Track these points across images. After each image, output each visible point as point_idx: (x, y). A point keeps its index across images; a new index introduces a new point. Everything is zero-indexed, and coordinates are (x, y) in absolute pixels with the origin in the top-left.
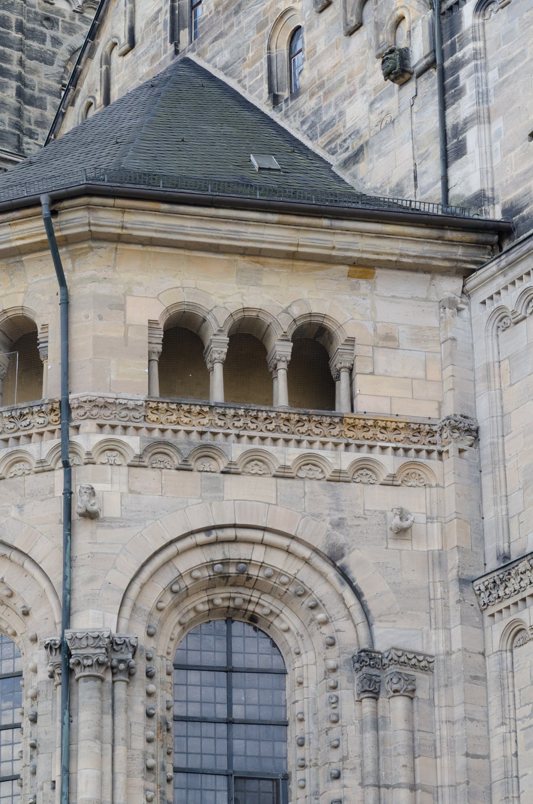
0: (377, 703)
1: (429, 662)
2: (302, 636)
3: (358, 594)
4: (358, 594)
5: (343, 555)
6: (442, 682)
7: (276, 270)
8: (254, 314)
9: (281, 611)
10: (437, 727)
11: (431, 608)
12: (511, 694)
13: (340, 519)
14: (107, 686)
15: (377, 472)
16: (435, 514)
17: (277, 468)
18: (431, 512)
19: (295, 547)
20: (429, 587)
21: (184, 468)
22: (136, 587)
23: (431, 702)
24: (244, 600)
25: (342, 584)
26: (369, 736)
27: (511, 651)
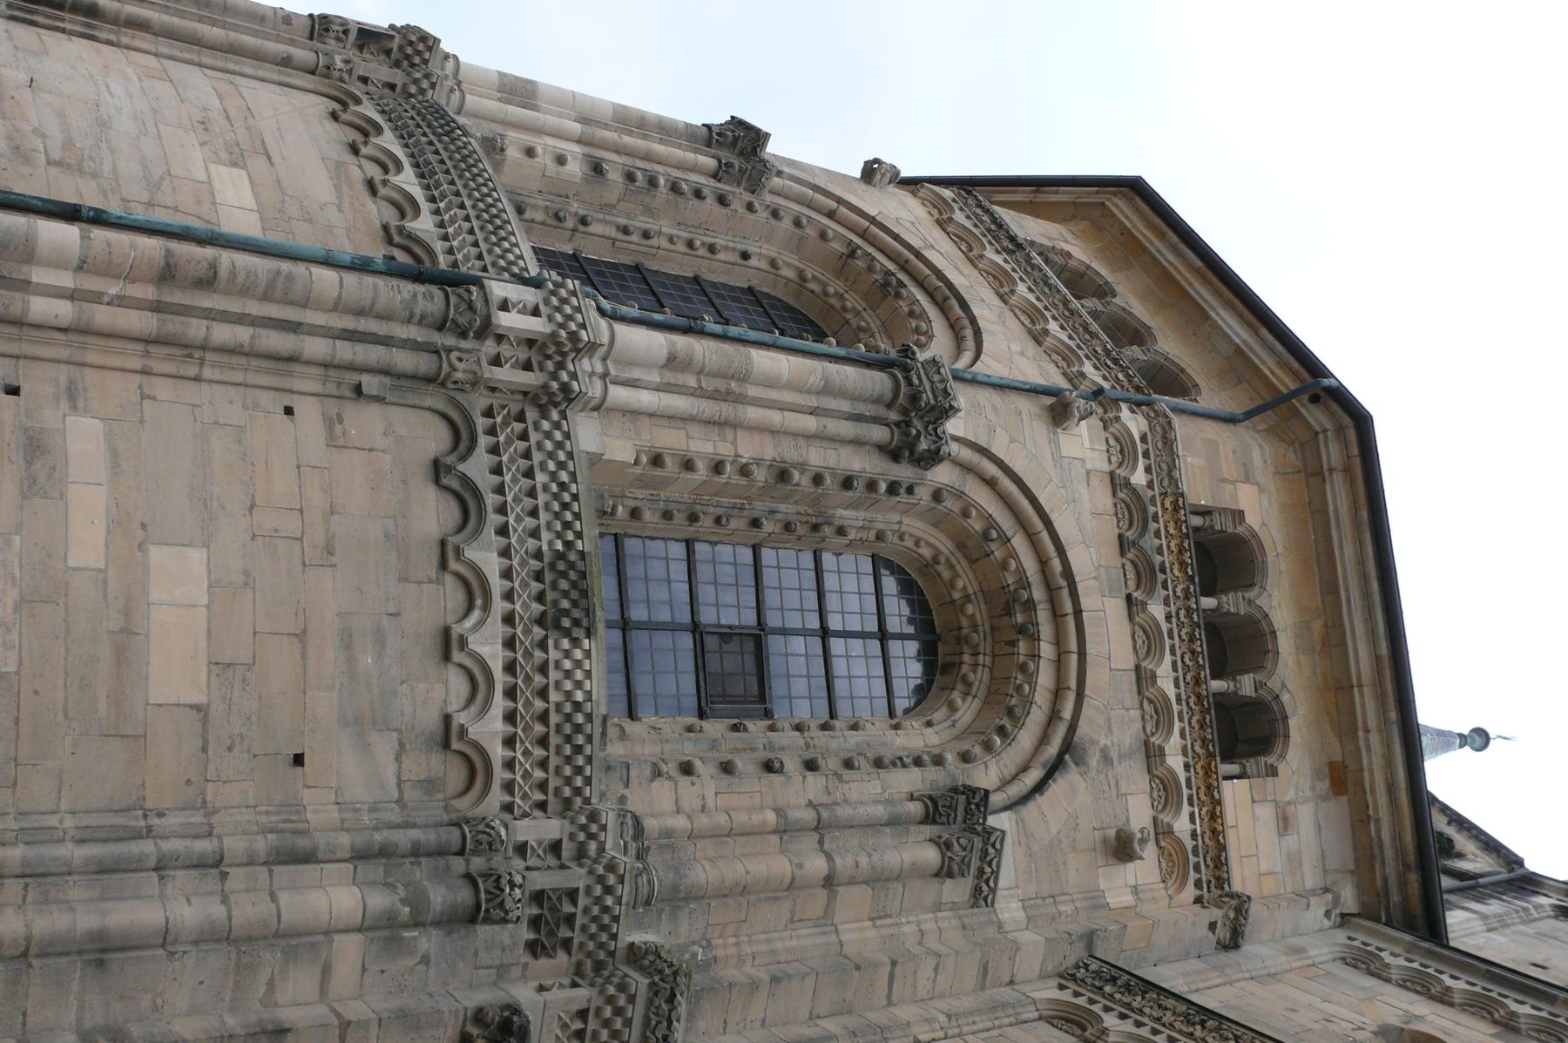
0: (921, 823)
1: (985, 899)
2: (953, 726)
3: (1040, 787)
5: (1077, 764)
6: (966, 921)
7: (1318, 670)
8: (1270, 647)
9: (975, 696)
10: (912, 918)
11: (1044, 899)
12: (990, 1024)
13: (1112, 761)
14: (880, 411)
15: (1168, 810)
16: (1140, 895)
17: (1150, 667)
18: (1142, 891)
20: (1067, 894)
21: (1123, 544)
22: (992, 470)
23: (938, 907)
24: (977, 645)
25: (1044, 766)
26: (880, 811)
27: (1040, 1018)
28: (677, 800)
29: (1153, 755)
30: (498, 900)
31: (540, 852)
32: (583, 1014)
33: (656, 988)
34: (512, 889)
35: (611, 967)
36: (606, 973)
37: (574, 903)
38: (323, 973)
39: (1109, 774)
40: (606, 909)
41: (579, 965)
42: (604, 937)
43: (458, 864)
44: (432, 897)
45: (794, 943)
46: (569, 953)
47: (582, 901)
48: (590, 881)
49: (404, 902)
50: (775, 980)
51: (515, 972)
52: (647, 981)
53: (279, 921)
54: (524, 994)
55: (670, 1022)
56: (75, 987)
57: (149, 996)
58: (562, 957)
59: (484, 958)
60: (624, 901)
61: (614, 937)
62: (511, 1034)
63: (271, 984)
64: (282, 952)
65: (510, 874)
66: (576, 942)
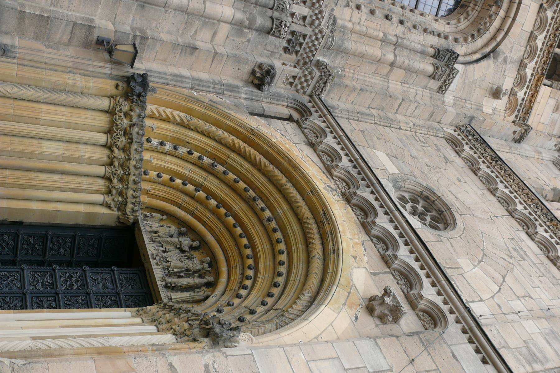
0: (431, 57)
1: (442, 91)
2: (457, 28)
3: (477, 61)
4: (477, 61)
5: (494, 58)
6: (433, 96)
10: (415, 88)
12: (426, 133)
16: (495, 112)
17: (536, 34)
18: (496, 111)
19: (502, 34)
20: (470, 101)
23: (425, 88)
25: (482, 54)
26: (419, 47)
27: (443, 138)
28: (351, 17)
29: (522, 66)
30: (279, 29)
31: (298, 18)
32: (294, 77)
33: (321, 78)
34: (285, 27)
35: (309, 65)
36: (307, 67)
37: (304, 39)
38: (214, 34)
39: (504, 66)
40: (314, 45)
41: (299, 61)
42: (310, 54)
43: (270, 12)
44: (257, 21)
45: (373, 80)
46: (297, 56)
47: (307, 39)
48: (312, 34)
49: (247, 19)
50: (362, 90)
51: (277, 55)
52: (319, 74)
53: (204, 11)
54: (277, 64)
55: (322, 90)
56: (133, 12)
57: (156, 22)
58: (294, 56)
59: (268, 47)
60: (321, 45)
61: (314, 55)
62: (269, 75)
63: (196, 32)
64: (202, 22)
65: (286, 22)
66: (300, 53)
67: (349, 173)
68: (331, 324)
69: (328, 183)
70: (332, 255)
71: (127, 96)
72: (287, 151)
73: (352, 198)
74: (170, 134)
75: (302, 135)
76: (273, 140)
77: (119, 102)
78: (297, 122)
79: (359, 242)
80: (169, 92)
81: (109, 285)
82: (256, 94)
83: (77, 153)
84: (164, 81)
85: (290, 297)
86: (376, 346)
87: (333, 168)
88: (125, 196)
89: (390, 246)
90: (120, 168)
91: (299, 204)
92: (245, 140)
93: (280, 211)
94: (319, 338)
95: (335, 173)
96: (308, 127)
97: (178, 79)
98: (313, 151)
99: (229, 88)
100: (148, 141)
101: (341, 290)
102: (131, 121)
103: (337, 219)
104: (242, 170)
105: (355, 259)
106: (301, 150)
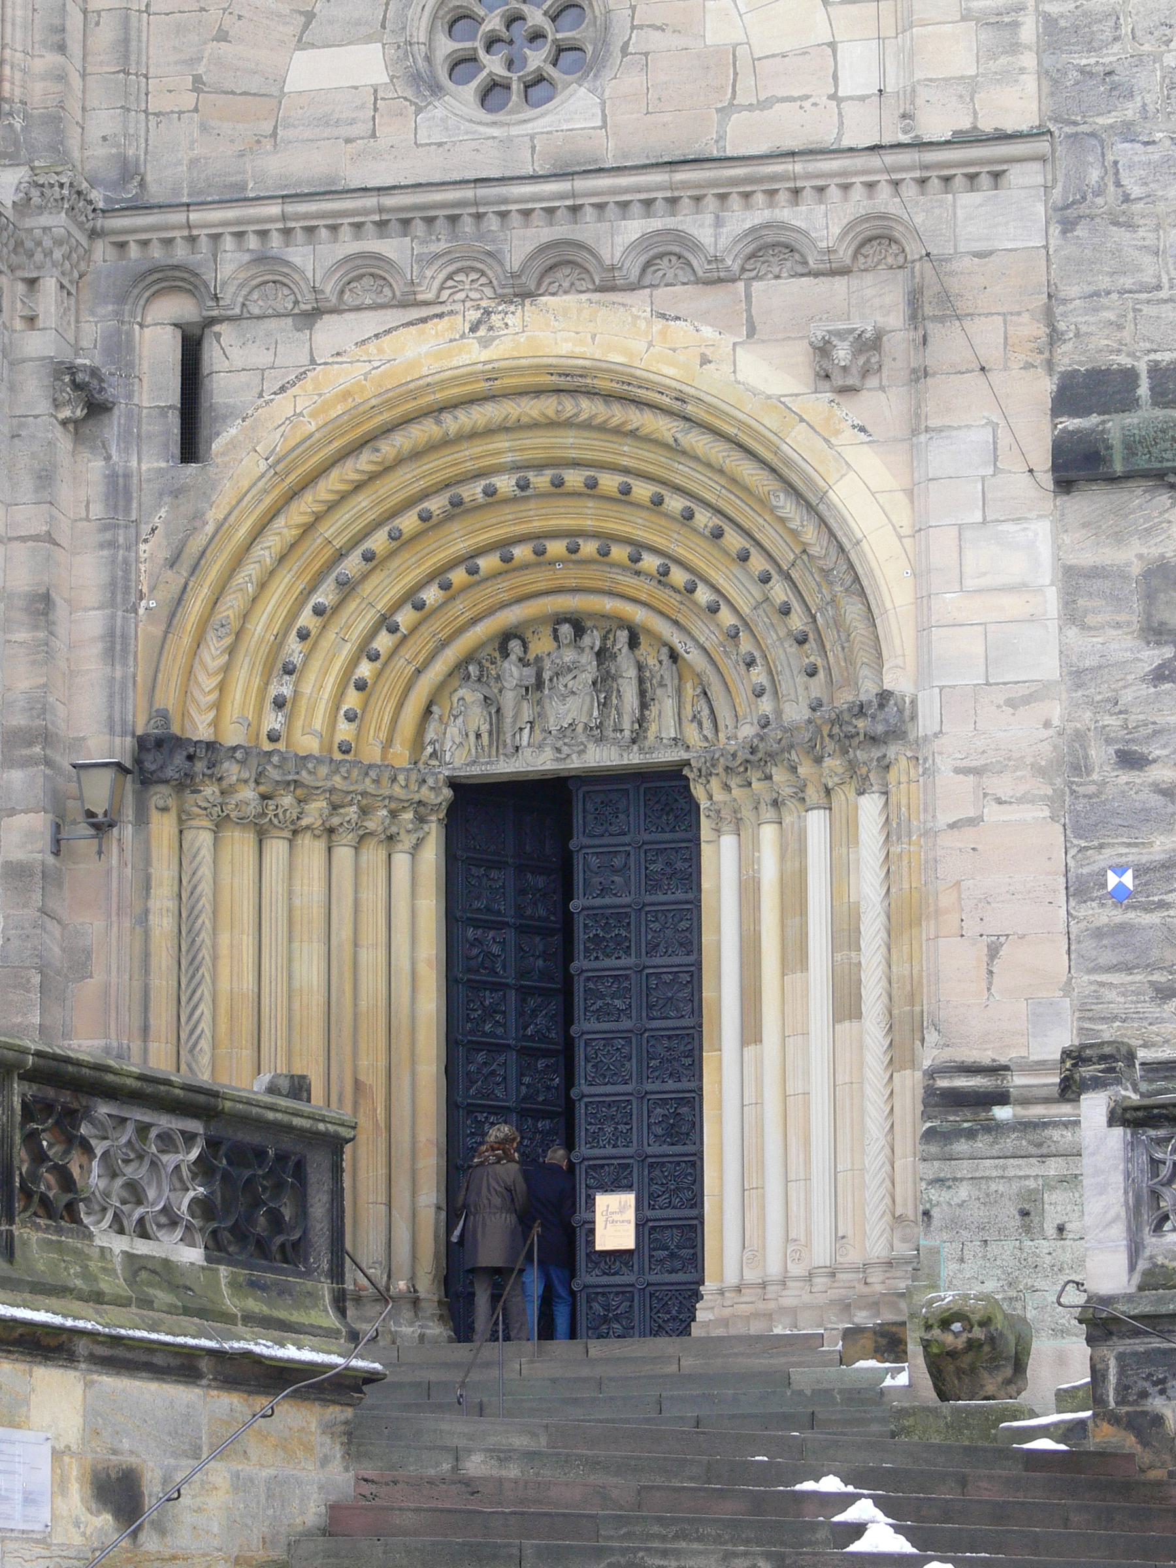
67: (437, 256)
68: (873, 494)
69: (461, 324)
70: (689, 407)
71: (185, 784)
72: (350, 403)
73: (522, 285)
74: (257, 682)
75: (272, 324)
76: (313, 427)
77: (206, 809)
78: (211, 321)
79: (659, 324)
80: (160, 676)
81: (618, 862)
82: (122, 421)
83: (315, 910)
84: (130, 685)
85: (766, 525)
86: (943, 434)
87: (415, 293)
88: (406, 805)
89: (677, 249)
90: (342, 811)
91: (514, 417)
92: (294, 494)
93: (508, 458)
94: (903, 532)
95: (430, 296)
96: (241, 299)
97: (118, 647)
98: (335, 317)
99: (121, 503)
100: (273, 737)
101: (793, 434)
102: (246, 781)
103: (588, 356)
104: (372, 516)
105: (710, 362)
106: (338, 354)
